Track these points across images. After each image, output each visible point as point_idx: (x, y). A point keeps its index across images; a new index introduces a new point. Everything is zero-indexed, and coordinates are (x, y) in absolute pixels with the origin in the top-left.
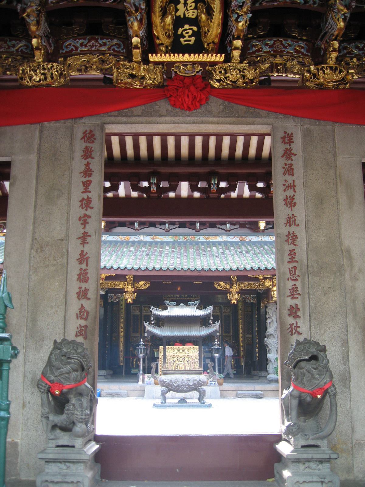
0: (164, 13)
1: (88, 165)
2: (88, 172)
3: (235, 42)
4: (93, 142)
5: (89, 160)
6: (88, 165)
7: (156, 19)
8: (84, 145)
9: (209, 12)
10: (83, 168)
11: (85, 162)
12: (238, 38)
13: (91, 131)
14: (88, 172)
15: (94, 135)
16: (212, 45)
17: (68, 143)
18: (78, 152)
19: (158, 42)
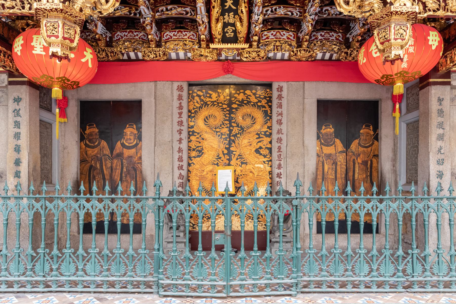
0: (217, 20)
1: (180, 103)
2: (181, 107)
3: (254, 37)
4: (183, 92)
5: (181, 101)
6: (180, 103)
7: (213, 25)
8: (178, 93)
9: (241, 20)
10: (178, 105)
11: (179, 102)
12: (256, 35)
13: (181, 86)
14: (181, 107)
15: (182, 88)
16: (242, 39)
17: (170, 92)
18: (176, 97)
19: (214, 37)
